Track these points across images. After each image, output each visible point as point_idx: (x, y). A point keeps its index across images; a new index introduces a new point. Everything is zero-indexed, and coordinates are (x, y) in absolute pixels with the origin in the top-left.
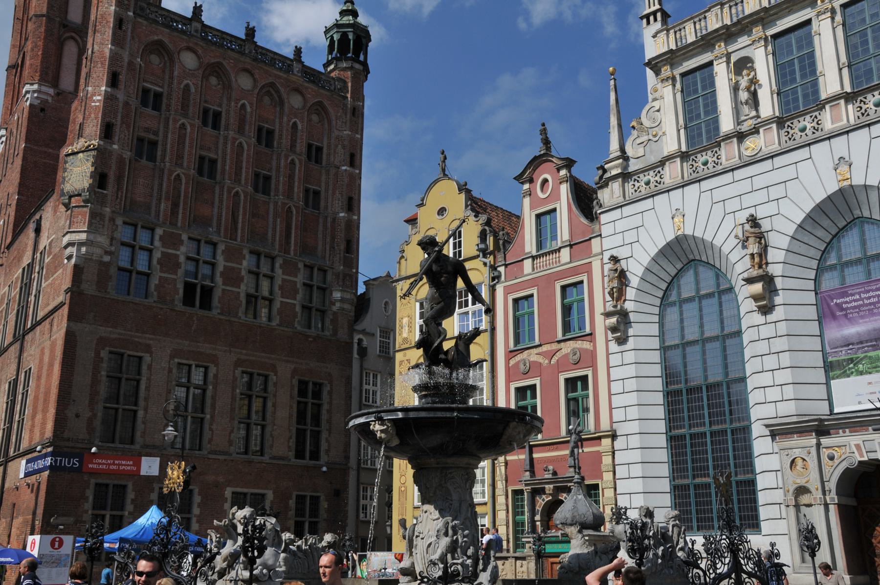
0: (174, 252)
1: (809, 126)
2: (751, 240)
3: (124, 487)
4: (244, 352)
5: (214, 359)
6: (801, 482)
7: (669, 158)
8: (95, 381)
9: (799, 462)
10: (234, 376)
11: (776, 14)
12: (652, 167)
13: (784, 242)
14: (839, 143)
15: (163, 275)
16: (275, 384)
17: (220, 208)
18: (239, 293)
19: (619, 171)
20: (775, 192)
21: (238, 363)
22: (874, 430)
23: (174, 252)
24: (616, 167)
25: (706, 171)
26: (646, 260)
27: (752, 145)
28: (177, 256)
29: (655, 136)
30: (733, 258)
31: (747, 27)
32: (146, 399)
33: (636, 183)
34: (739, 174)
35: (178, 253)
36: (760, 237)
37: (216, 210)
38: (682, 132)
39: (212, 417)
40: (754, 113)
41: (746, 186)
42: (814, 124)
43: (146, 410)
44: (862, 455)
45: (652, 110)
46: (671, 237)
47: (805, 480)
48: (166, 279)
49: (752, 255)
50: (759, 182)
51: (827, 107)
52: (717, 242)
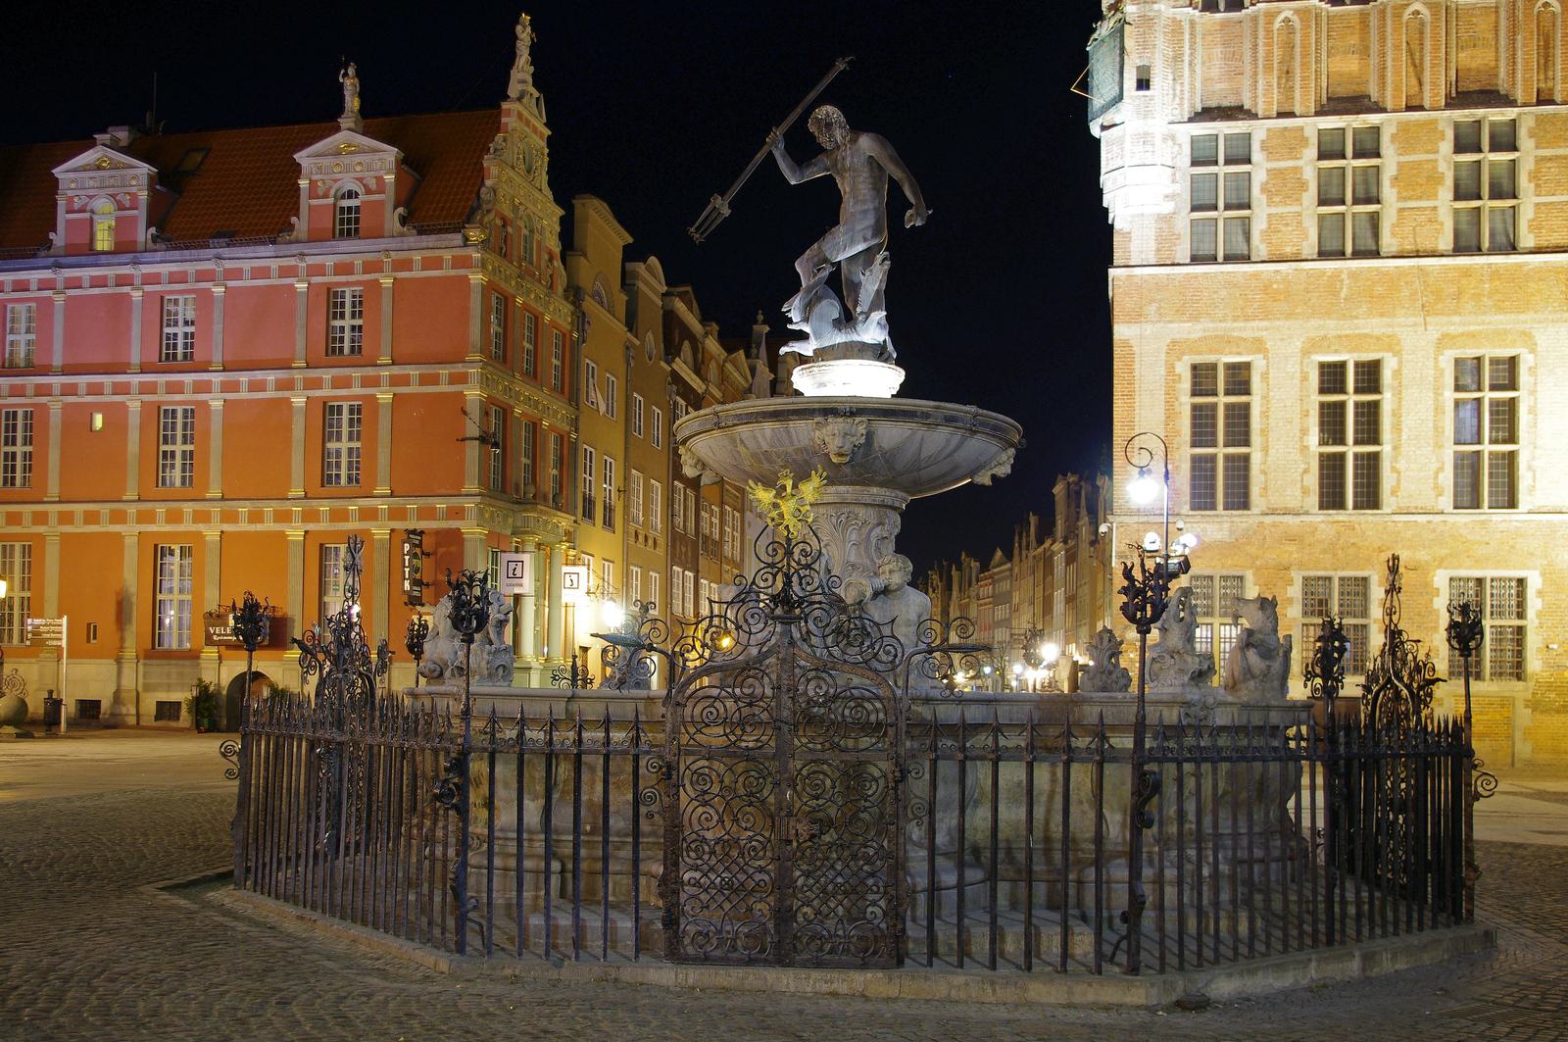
0: (1290, 163)
3: (1241, 578)
4: (1456, 319)
5: (1392, 344)
8: (1170, 415)
10: (1436, 367)
15: (1273, 210)
16: (1532, 370)
17: (1383, 55)
18: (1435, 208)
21: (1443, 342)
23: (1290, 163)
28: (1297, 170)
32: (1264, 432)
35: (1299, 163)
37: (1374, 61)
39: (1395, 448)
43: (1265, 450)
48: (1281, 216)
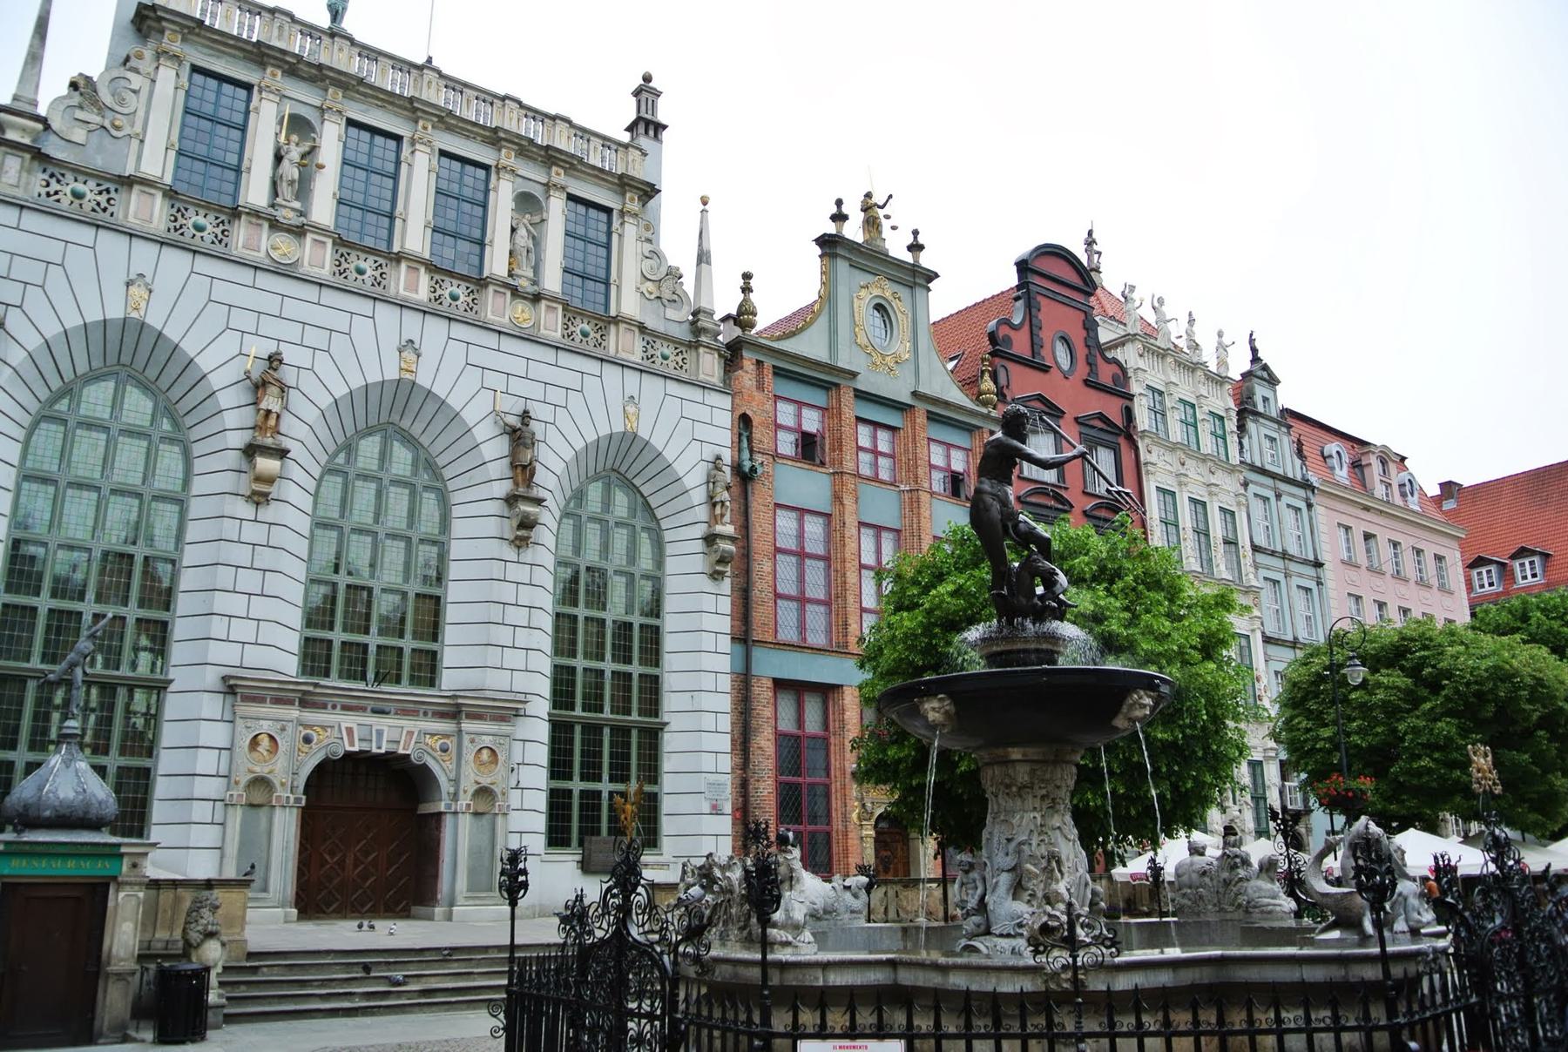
1: (369, 272)
2: (274, 390)
6: (261, 770)
7: (144, 182)
9: (265, 742)
11: (365, 95)
12: (100, 176)
13: (311, 415)
14: (412, 320)
19: (27, 141)
20: (314, 337)
22: (375, 711)
24: (24, 129)
25: (197, 240)
26: (52, 329)
27: (284, 247)
29: (118, 128)
30: (226, 399)
31: (323, 80)
33: (53, 182)
34: (264, 280)
36: (283, 388)
38: (172, 154)
40: (297, 205)
41: (270, 304)
42: (377, 274)
44: (352, 744)
45: (123, 82)
46: (115, 312)
47: (266, 770)
49: (268, 412)
50: (291, 308)
51: (403, 265)
52: (205, 363)
